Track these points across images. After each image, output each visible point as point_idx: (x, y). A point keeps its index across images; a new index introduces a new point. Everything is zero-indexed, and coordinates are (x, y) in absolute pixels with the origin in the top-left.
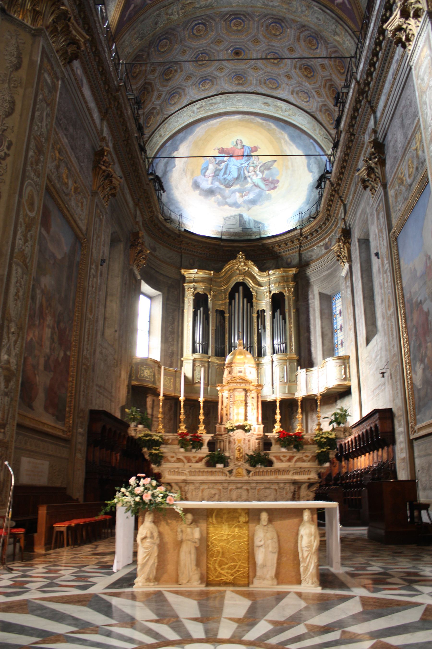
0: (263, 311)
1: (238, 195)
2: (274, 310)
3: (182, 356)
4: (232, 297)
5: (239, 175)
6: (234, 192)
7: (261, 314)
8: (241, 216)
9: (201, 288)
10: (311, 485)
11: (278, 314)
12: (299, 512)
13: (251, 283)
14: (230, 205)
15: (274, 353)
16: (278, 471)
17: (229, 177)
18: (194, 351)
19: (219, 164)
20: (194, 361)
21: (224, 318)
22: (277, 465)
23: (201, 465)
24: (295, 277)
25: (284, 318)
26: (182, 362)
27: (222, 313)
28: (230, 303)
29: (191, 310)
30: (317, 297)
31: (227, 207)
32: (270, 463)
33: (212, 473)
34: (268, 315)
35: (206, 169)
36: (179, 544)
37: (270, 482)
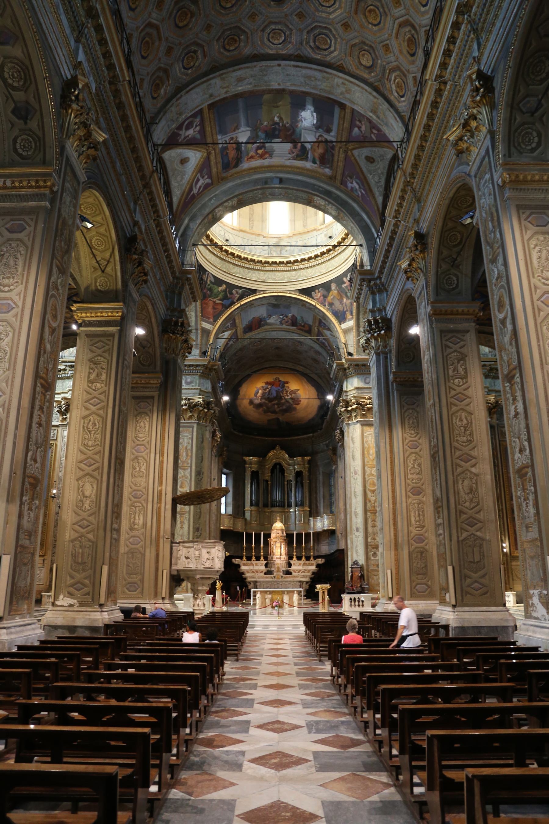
0: (291, 481)
1: (276, 406)
2: (297, 482)
3: (244, 508)
4: (272, 471)
5: (277, 395)
6: (274, 404)
7: (289, 482)
8: (278, 419)
9: (255, 467)
10: (307, 582)
11: (299, 484)
12: (293, 591)
13: (284, 464)
14: (272, 412)
15: (296, 506)
16: (294, 577)
17: (271, 397)
18: (251, 505)
19: (265, 389)
20: (251, 511)
21: (268, 484)
22: (294, 574)
23: (262, 574)
24: (309, 462)
25: (302, 486)
26: (244, 511)
27: (267, 481)
28: (271, 475)
29: (250, 481)
30: (321, 474)
31: (269, 414)
32: (291, 573)
33: (267, 578)
34: (293, 483)
35: (258, 393)
36: (266, 599)
37: (291, 582)
